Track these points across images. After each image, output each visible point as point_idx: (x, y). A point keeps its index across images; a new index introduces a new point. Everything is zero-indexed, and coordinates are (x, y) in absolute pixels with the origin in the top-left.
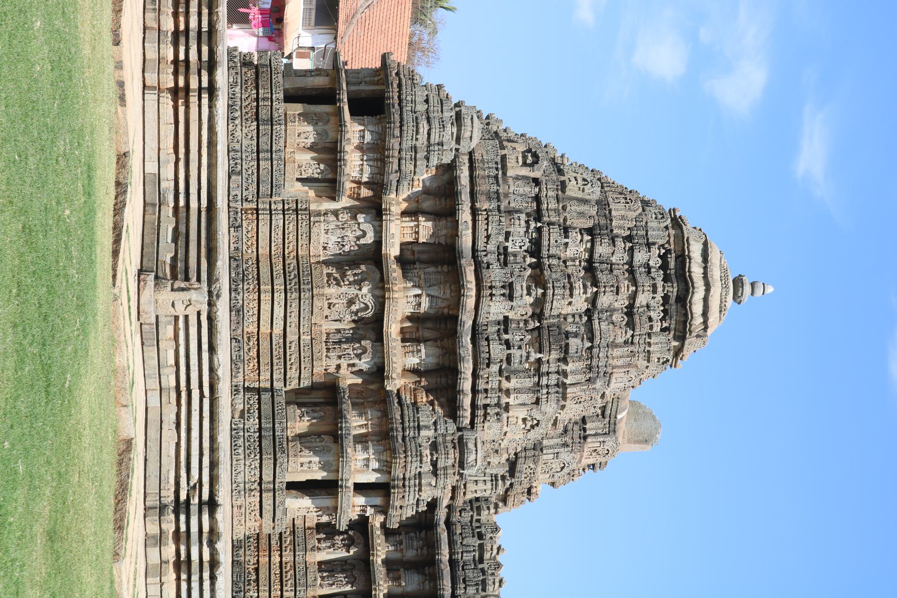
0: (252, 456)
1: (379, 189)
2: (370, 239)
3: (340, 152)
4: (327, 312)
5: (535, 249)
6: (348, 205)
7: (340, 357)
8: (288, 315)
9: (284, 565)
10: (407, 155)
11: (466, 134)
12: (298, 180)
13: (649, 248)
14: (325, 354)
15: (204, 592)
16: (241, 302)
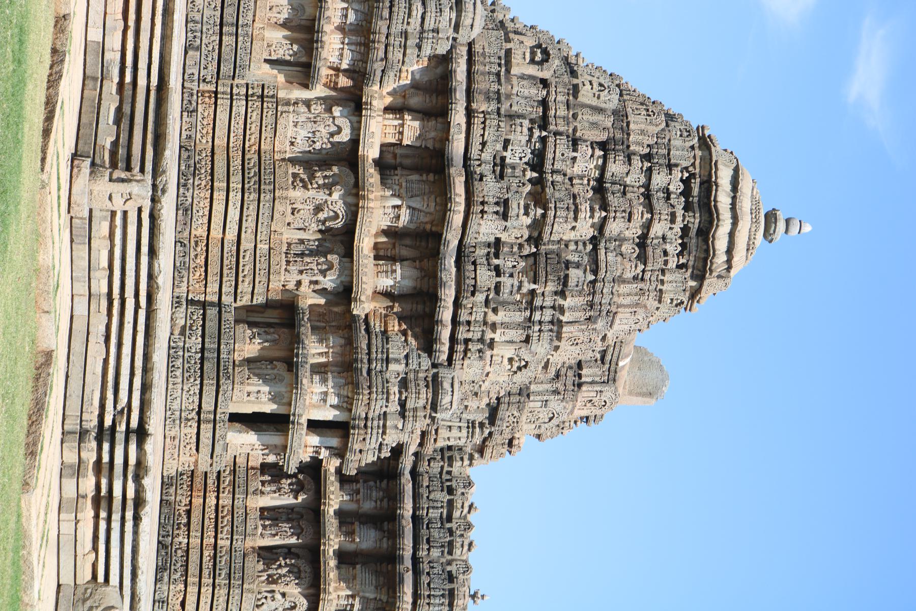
0: (192, 380)
1: (360, 79)
2: (345, 136)
3: (318, 32)
4: (289, 218)
5: (538, 162)
6: (323, 95)
7: (301, 272)
8: (244, 218)
9: (220, 509)
10: (396, 41)
11: (466, 21)
12: (266, 61)
13: (671, 170)
14: (284, 267)
15: (126, 534)
16: (190, 200)
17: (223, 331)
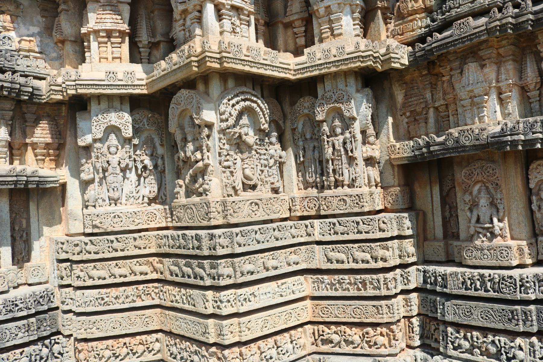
2: (123, 120)
4: (264, 192)
7: (351, 160)
14: (347, 190)
17: (492, 294)
